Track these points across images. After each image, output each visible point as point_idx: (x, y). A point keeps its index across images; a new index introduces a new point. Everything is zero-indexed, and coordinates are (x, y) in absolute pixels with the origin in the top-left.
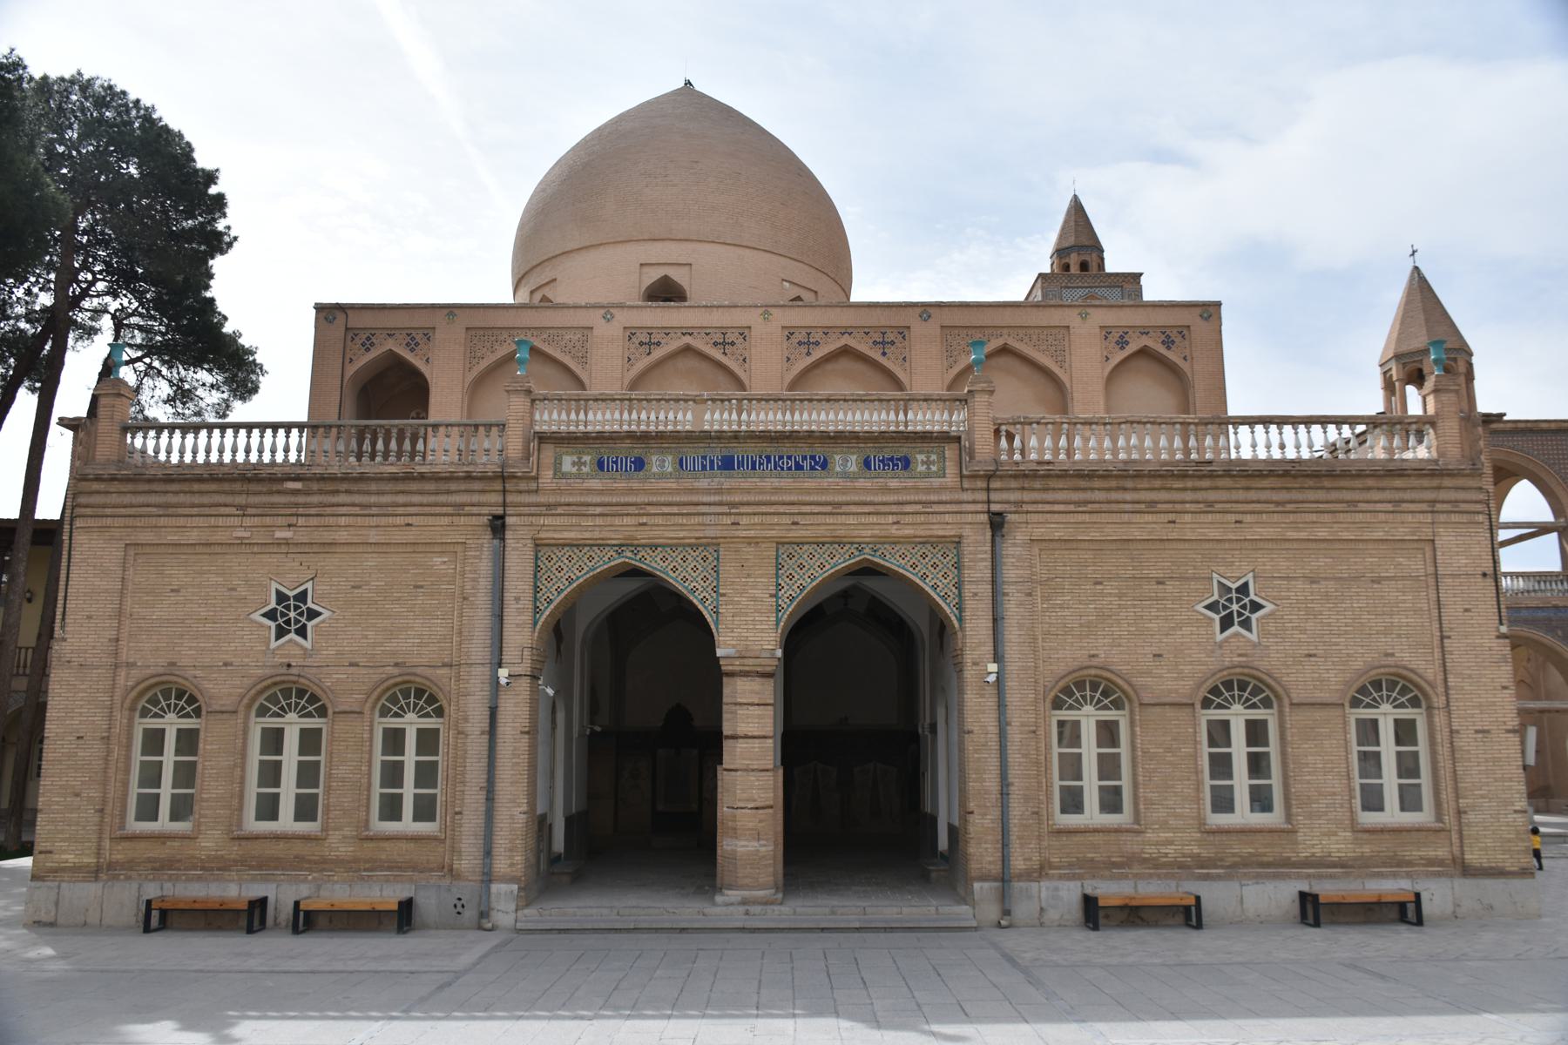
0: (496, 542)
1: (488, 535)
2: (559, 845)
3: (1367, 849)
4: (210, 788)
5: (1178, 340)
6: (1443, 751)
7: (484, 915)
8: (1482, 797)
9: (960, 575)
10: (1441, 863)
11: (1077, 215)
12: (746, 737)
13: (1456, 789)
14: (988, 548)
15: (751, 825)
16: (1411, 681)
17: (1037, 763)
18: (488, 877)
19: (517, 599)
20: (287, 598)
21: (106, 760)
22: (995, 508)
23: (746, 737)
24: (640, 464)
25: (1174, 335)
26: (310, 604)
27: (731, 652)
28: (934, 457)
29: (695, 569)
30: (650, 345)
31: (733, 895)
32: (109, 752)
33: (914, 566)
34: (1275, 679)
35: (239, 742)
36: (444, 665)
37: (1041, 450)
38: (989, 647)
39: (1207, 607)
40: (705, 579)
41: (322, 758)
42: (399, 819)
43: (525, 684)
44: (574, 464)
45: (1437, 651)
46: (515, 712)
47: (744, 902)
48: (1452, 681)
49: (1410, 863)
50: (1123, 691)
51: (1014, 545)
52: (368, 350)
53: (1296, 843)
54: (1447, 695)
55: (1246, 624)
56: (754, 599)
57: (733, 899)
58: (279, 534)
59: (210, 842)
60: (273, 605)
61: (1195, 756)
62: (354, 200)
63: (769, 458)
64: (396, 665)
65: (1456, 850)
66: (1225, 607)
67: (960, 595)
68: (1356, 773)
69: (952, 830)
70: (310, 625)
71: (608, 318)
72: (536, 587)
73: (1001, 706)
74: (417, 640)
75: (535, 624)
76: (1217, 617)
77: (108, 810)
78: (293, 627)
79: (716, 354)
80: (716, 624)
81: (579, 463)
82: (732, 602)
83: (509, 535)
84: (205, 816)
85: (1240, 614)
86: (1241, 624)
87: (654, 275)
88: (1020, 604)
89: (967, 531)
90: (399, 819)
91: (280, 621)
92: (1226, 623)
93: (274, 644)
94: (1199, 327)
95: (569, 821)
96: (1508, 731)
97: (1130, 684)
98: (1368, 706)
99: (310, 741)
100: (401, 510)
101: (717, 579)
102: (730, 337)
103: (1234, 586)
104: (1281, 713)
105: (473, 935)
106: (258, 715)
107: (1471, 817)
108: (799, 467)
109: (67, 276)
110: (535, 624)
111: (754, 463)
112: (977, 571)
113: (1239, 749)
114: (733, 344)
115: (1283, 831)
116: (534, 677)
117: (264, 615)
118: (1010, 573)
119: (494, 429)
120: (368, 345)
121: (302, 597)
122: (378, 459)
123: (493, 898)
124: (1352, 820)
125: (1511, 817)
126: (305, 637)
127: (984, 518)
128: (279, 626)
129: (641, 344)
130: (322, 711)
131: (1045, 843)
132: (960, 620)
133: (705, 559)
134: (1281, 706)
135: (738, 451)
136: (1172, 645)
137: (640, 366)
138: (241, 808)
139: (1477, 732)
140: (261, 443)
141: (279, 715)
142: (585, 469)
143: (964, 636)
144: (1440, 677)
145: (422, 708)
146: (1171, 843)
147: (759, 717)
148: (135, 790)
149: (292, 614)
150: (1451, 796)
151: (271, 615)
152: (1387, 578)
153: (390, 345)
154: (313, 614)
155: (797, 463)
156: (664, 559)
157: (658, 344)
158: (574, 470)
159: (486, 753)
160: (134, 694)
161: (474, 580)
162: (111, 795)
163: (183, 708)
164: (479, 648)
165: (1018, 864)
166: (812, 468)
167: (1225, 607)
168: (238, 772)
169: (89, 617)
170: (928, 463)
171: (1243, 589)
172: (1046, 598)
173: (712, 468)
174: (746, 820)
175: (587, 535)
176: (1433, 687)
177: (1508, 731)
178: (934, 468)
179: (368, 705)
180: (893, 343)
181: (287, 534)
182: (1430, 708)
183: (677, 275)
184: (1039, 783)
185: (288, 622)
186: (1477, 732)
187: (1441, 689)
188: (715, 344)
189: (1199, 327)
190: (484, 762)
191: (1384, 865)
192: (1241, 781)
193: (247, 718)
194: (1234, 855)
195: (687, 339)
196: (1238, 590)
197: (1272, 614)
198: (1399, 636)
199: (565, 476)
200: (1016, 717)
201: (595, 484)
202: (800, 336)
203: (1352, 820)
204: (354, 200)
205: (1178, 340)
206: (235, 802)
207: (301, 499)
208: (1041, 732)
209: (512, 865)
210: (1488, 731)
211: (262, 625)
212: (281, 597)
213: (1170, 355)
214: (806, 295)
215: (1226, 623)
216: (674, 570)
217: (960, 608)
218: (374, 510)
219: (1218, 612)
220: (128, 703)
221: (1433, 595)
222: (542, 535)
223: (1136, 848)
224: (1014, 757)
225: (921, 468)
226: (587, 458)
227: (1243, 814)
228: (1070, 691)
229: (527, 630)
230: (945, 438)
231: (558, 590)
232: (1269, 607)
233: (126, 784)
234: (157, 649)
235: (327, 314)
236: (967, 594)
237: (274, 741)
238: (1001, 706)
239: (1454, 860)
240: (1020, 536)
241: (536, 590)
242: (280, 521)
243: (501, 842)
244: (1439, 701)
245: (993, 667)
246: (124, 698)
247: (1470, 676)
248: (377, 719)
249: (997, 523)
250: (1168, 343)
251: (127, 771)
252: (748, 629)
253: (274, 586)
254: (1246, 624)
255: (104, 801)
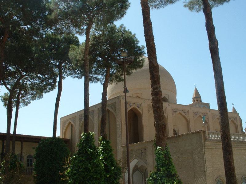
11: (197, 92)
30: (175, 111)
52: (130, 106)
64: (243, 174)
79: (184, 114)
100: (241, 149)
102: (186, 112)
129: (174, 111)
153: (134, 106)
157: (176, 112)
195: (180, 111)
218: (238, 148)
250: (234, 119)
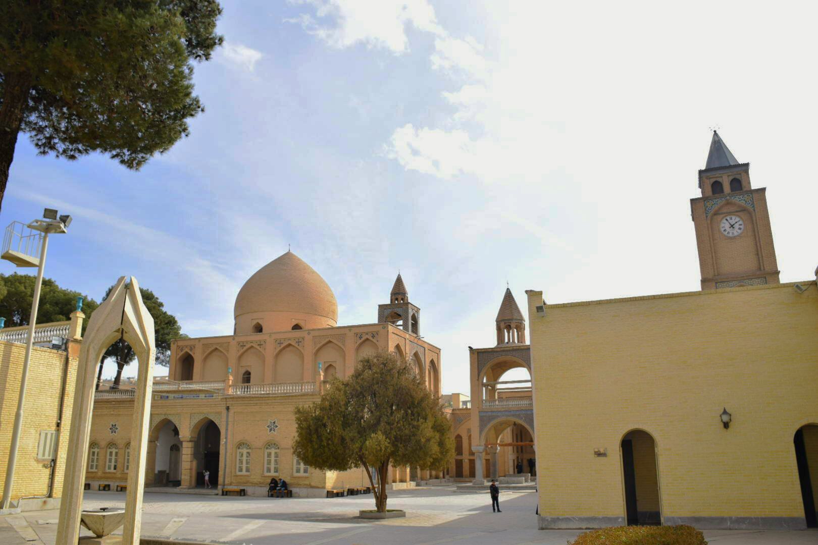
59: (100, 474)
87: (255, 322)
112: (224, 419)
118: (230, 419)
120: (182, 350)
137: (242, 351)
165: (226, 482)
174: (184, 472)
214: (302, 324)
224: (228, 460)
228: (240, 445)
231: (155, 424)
249: (228, 408)
250: (373, 337)
252: (186, 432)
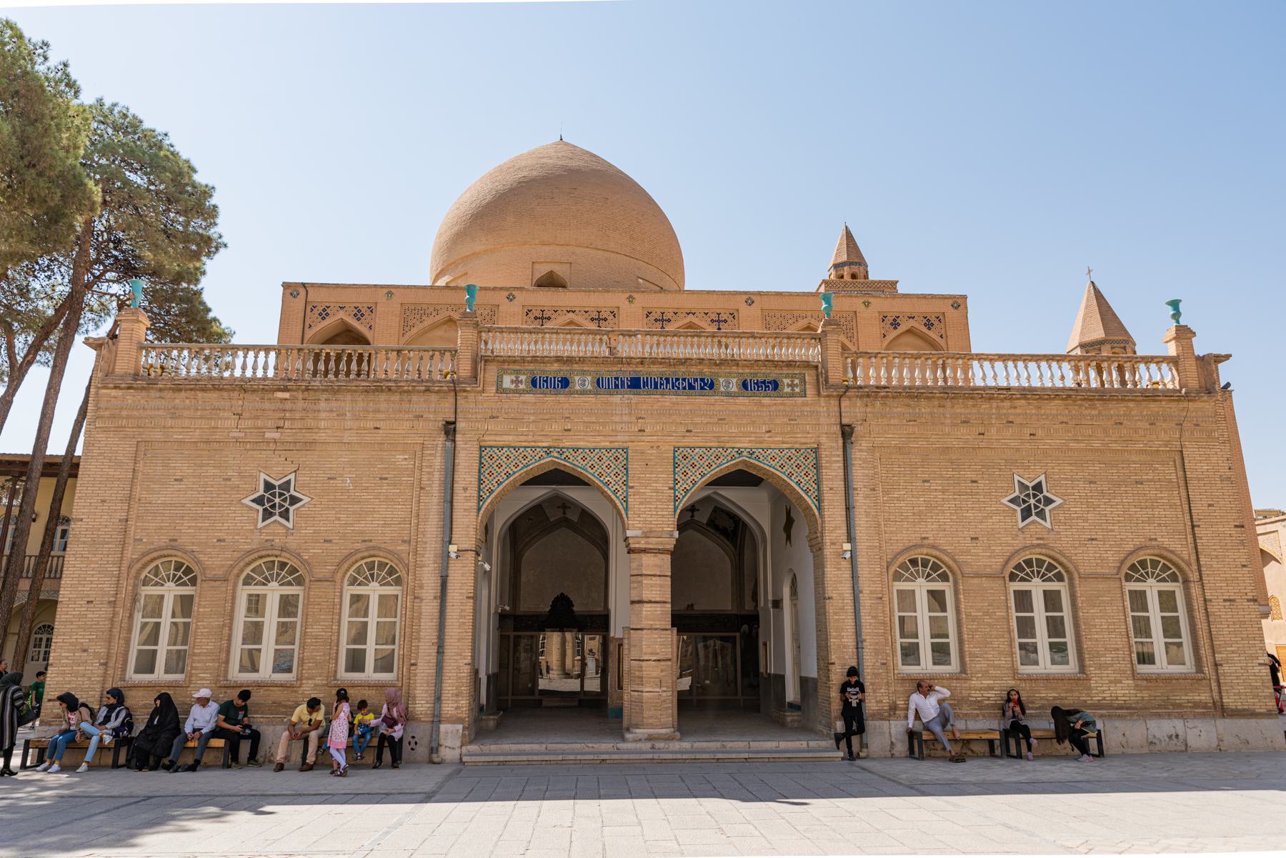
0: (449, 444)
1: (442, 438)
2: (483, 700)
3: (1145, 694)
4: (203, 644)
5: (936, 323)
6: (1200, 616)
7: (434, 750)
8: (1233, 652)
9: (818, 473)
10: (1205, 706)
12: (650, 602)
13: (1212, 646)
14: (840, 452)
15: (654, 674)
16: (1170, 561)
17: (884, 623)
18: (437, 719)
19: (465, 489)
20: (273, 487)
21: (112, 620)
22: (845, 421)
23: (650, 602)
24: (565, 383)
25: (933, 320)
26: (292, 492)
27: (638, 533)
28: (797, 381)
29: (609, 467)
31: (641, 732)
32: (115, 614)
33: (782, 466)
34: (1066, 557)
35: (228, 605)
36: (404, 541)
37: (878, 378)
38: (844, 530)
39: (1011, 501)
40: (617, 475)
41: (298, 620)
42: (362, 670)
43: (470, 556)
44: (512, 382)
45: (1190, 537)
46: (462, 577)
47: (650, 738)
48: (1203, 560)
49: (1180, 706)
50: (949, 567)
51: (860, 450)
52: (323, 319)
53: (1090, 688)
54: (1200, 571)
55: (1041, 514)
56: (657, 491)
57: (640, 736)
58: (268, 435)
60: (261, 492)
61: (1008, 619)
62: (313, 206)
63: (667, 380)
65: (1216, 696)
66: (1024, 502)
67: (819, 489)
68: (1132, 633)
69: (804, 682)
70: (292, 509)
71: (511, 298)
72: (480, 480)
73: (854, 577)
74: (383, 521)
75: (479, 509)
76: (1019, 509)
77: (111, 664)
78: (277, 511)
80: (626, 509)
81: (517, 382)
82: (639, 493)
83: (459, 437)
84: (196, 668)
85: (1036, 507)
86: (1037, 514)
87: (542, 270)
88: (867, 497)
89: (823, 440)
90: (362, 670)
91: (267, 506)
92: (1026, 513)
93: (260, 525)
94: (951, 314)
95: (489, 677)
96: (1249, 600)
97: (955, 561)
98: (1138, 580)
99: (287, 605)
101: (627, 475)
103: (1031, 485)
104: (1072, 586)
105: (427, 770)
106: (244, 584)
107: (1225, 669)
108: (691, 387)
109: (81, 265)
110: (479, 509)
111: (656, 384)
113: (1039, 615)
114: (605, 320)
115: (1079, 679)
116: (478, 554)
117: (253, 501)
118: (858, 473)
119: (448, 354)
120: (324, 315)
121: (286, 486)
122: (352, 376)
123: (442, 735)
124: (1133, 670)
125: (1257, 669)
126: (288, 520)
127: (837, 429)
128: (265, 510)
129: (536, 318)
130: (299, 581)
131: (892, 689)
132: (819, 509)
133: (617, 459)
134: (1071, 579)
135: (643, 372)
136: (983, 531)
138: (227, 662)
139: (1225, 600)
140: (256, 361)
141: (264, 584)
142: (522, 387)
143: (823, 522)
144: (1193, 557)
145: (384, 578)
146: (992, 689)
147: (661, 586)
148: (135, 647)
149: (277, 500)
150: (1209, 652)
151: (259, 501)
152: (1148, 480)
153: (341, 315)
154: (294, 500)
155: (690, 384)
156: (584, 459)
158: (513, 387)
159: (437, 614)
160: (138, 566)
161: (429, 473)
162: (114, 651)
163: (180, 578)
164: (432, 527)
166: (702, 388)
167: (1024, 502)
168: (226, 631)
169: (103, 501)
170: (792, 386)
171: (1038, 487)
172: (886, 492)
173: (623, 386)
174: (652, 671)
175: (522, 438)
176: (1189, 564)
177: (1249, 600)
178: (797, 390)
179: (339, 575)
180: (725, 321)
181: (276, 435)
182: (1186, 581)
183: (561, 271)
184: (886, 639)
185: (273, 506)
186: (1225, 600)
187: (1195, 567)
188: (592, 319)
189: (951, 314)
190: (435, 622)
191: (1160, 706)
192: (1042, 638)
193: (235, 585)
194: (1042, 698)
196: (1034, 488)
197: (1060, 506)
198: (1160, 525)
199: (505, 391)
200: (866, 586)
201: (529, 398)
202: (658, 316)
203: (1133, 670)
204: (313, 206)
205: (936, 323)
206: (223, 655)
207: (288, 405)
208: (886, 599)
209: (457, 708)
210: (1233, 600)
211: (251, 508)
212: (268, 486)
213: (930, 333)
215: (1026, 513)
216: (592, 467)
217: (819, 499)
219: (1019, 505)
220: (133, 572)
221: (1184, 494)
222: (486, 438)
223: (965, 693)
224: (866, 619)
225: (787, 390)
226: (523, 378)
227: (1045, 664)
229: (474, 513)
230: (807, 365)
231: (499, 483)
232: (1059, 501)
233: (128, 642)
234: (161, 528)
235: (291, 290)
236: (825, 488)
237: (256, 604)
238: (854, 577)
239: (1214, 703)
240: (864, 444)
241: (480, 482)
242: (270, 424)
243: (449, 687)
244: (1194, 576)
245: (847, 546)
246: (130, 567)
247: (1217, 557)
248: (346, 587)
249: (847, 433)
250: (929, 325)
251: (130, 630)
253: (263, 476)
254: (1041, 514)
255: (108, 655)
